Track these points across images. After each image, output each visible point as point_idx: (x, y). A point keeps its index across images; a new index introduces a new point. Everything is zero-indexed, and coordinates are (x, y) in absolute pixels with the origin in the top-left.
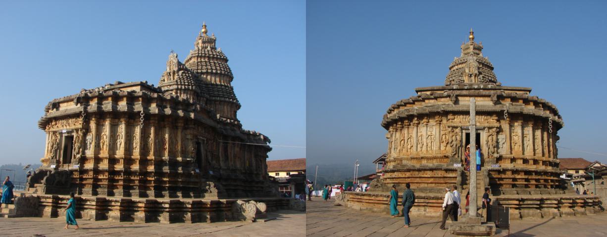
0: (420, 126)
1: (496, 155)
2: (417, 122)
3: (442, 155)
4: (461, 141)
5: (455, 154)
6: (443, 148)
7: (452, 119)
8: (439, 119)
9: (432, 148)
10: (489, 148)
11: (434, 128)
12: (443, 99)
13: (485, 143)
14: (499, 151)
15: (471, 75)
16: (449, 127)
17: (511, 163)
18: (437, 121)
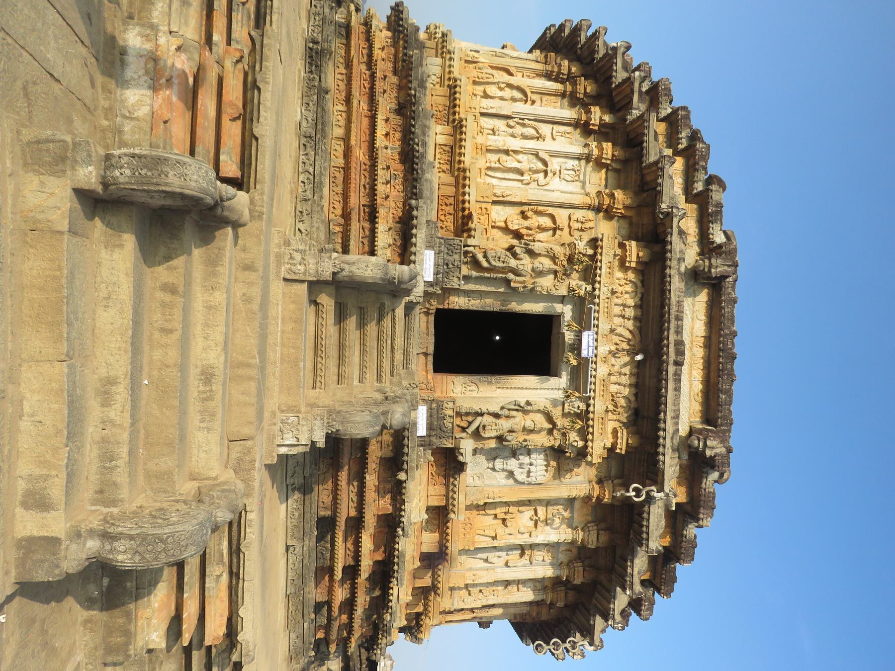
0: (576, 134)
1: (467, 445)
3: (473, 207)
4: (532, 294)
6: (499, 214)
10: (496, 416)
11: (575, 187)
13: (521, 397)
14: (481, 459)
18: (612, 196)
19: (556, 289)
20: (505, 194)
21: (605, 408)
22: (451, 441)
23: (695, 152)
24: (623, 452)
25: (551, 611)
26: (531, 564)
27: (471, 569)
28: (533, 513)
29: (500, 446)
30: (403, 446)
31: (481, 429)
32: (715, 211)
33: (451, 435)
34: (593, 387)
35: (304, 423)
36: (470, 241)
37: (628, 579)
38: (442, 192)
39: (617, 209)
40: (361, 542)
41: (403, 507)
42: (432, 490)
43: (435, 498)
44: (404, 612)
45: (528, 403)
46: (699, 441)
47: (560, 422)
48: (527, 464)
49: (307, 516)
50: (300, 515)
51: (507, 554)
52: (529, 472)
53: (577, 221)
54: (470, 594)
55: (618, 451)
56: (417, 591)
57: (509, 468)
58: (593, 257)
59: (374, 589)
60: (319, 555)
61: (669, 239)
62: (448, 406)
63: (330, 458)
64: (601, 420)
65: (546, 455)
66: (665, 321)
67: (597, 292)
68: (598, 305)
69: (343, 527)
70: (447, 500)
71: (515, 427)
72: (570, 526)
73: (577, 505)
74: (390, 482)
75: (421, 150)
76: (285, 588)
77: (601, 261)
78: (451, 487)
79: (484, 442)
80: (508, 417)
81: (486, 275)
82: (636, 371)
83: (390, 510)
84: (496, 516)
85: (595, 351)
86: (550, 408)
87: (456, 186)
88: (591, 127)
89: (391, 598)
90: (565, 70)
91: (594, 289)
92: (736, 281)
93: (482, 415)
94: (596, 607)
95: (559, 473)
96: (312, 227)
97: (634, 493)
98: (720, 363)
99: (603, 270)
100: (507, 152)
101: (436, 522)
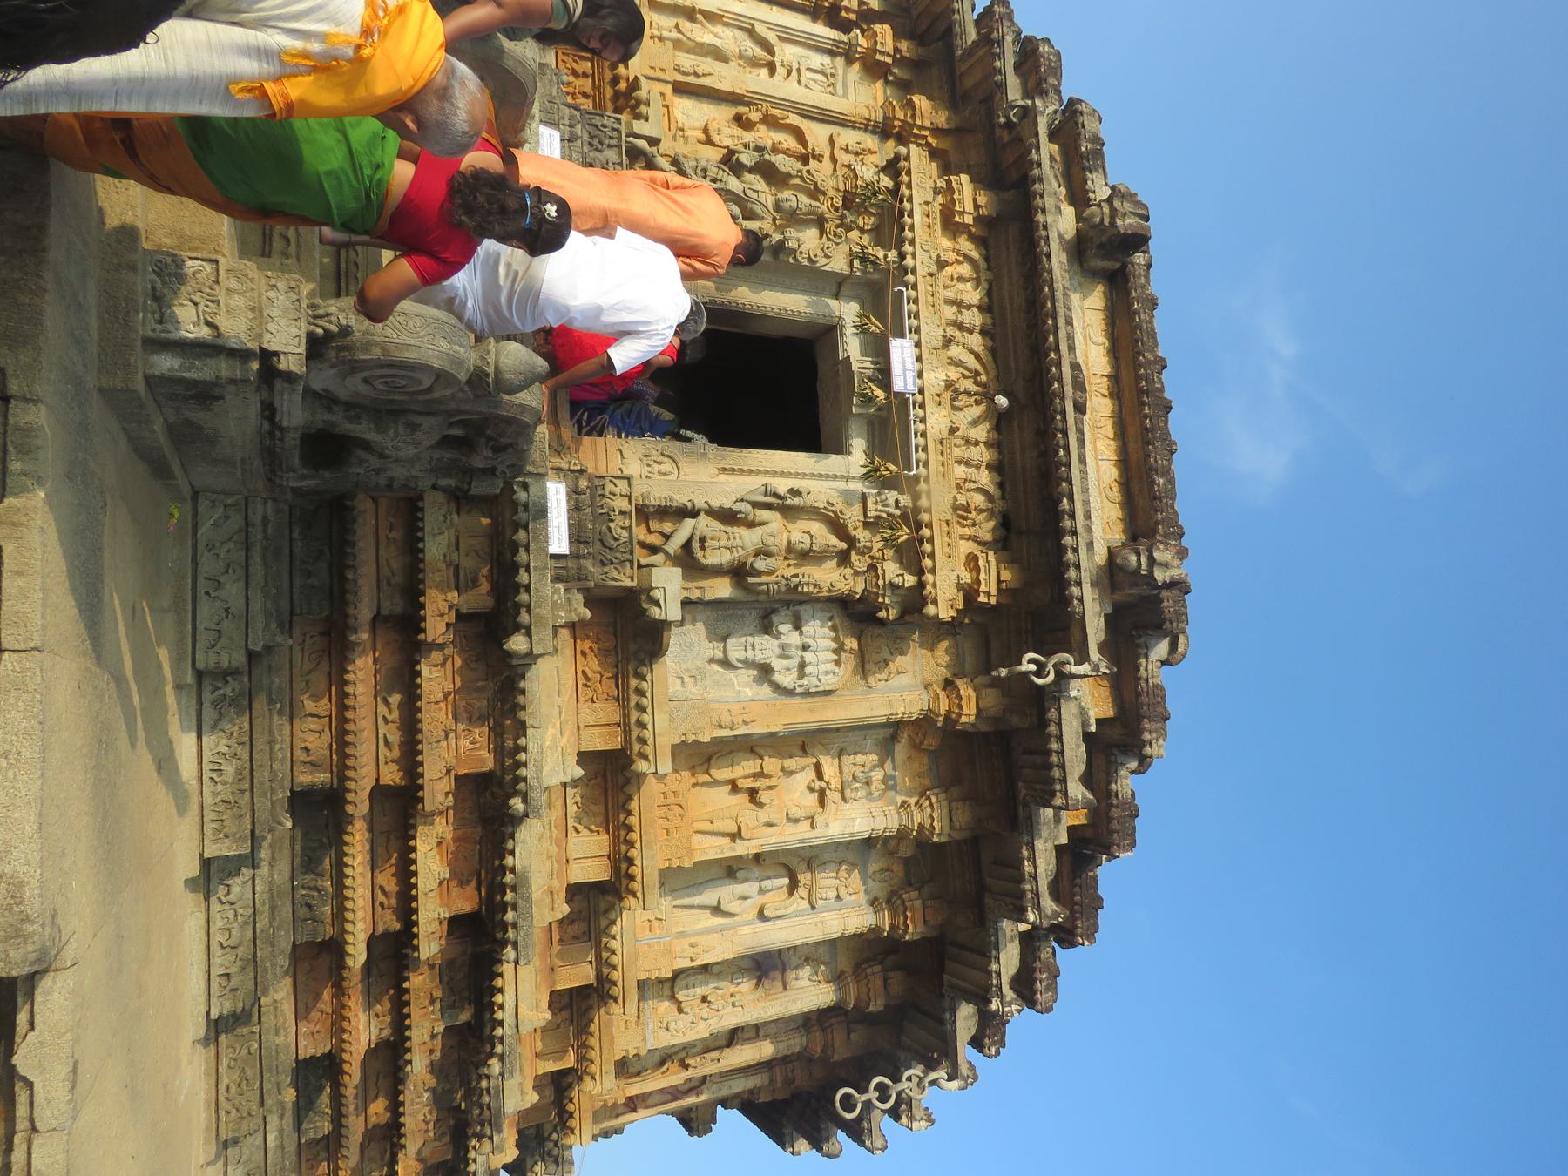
1: (669, 585)
10: (728, 517)
19: (827, 257)
20: (700, 71)
21: (951, 501)
22: (628, 571)
23: (1037, 61)
24: (993, 601)
25: (853, 1036)
26: (813, 908)
27: (682, 934)
28: (812, 774)
29: (740, 595)
30: (515, 568)
31: (696, 545)
32: (1092, 149)
33: (628, 556)
34: (922, 455)
35: (233, 284)
36: (639, 127)
37: (1028, 887)
39: (921, 128)
40: (414, 862)
41: (522, 741)
42: (588, 714)
43: (596, 730)
46: (1138, 555)
47: (862, 535)
48: (797, 648)
49: (262, 775)
50: (239, 772)
51: (761, 891)
52: (802, 665)
53: (847, 150)
54: (680, 1011)
55: (982, 599)
57: (760, 656)
58: (895, 192)
60: (303, 912)
61: (1035, 157)
62: (617, 490)
63: (321, 634)
64: (945, 528)
65: (834, 628)
66: (1047, 315)
67: (909, 261)
68: (915, 287)
70: (627, 733)
74: (480, 690)
76: (202, 999)
77: (910, 200)
78: (634, 699)
79: (700, 584)
80: (751, 525)
82: (994, 435)
83: (488, 762)
84: (734, 787)
85: (919, 382)
88: (843, 14)
89: (499, 1015)
91: (902, 256)
92: (1149, 265)
93: (693, 513)
94: (952, 986)
95: (865, 665)
97: (1033, 667)
98: (1146, 416)
99: (917, 217)
101: (600, 809)
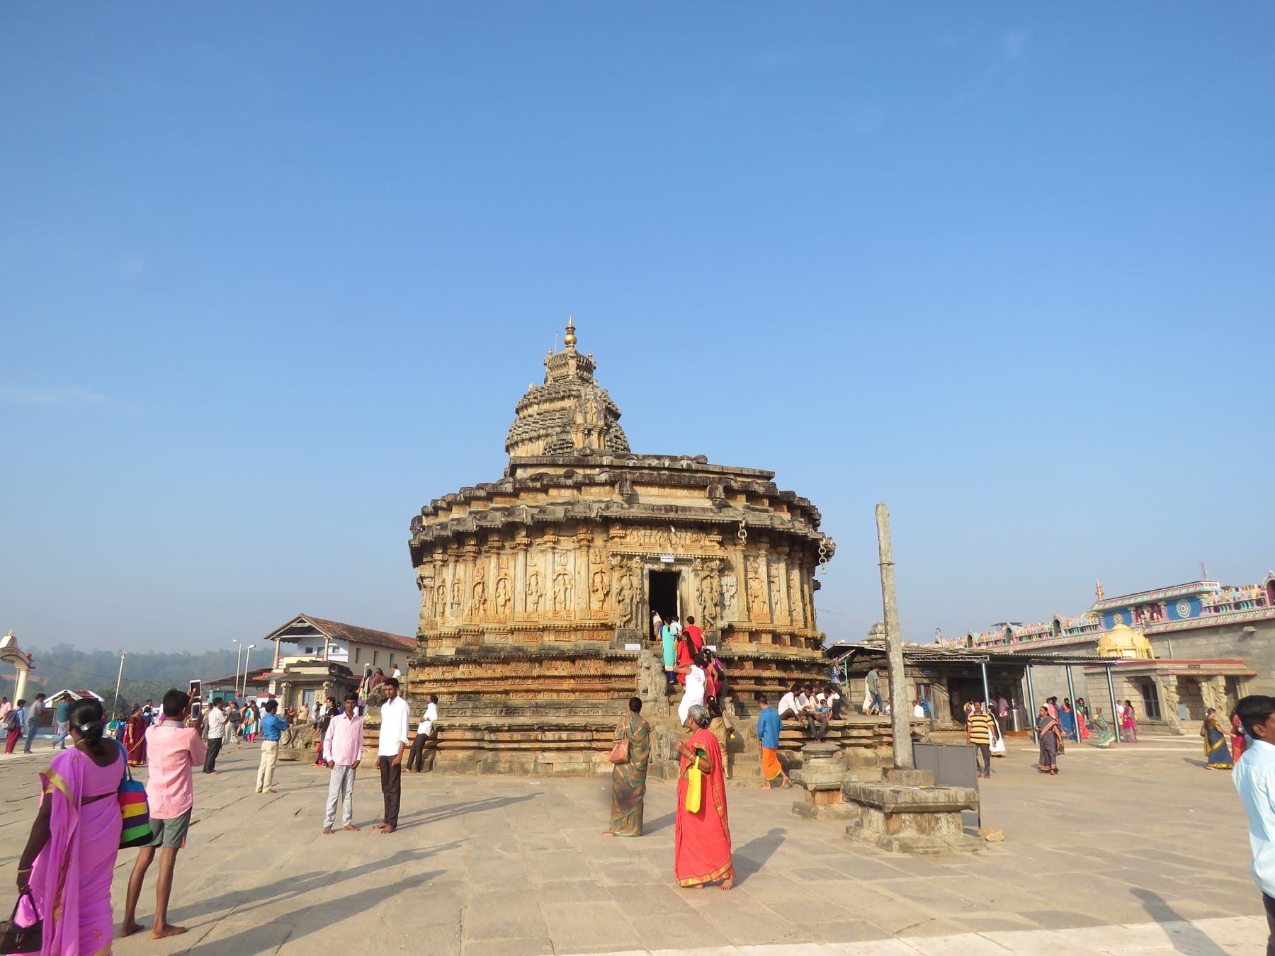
2: (525, 541)
5: (629, 621)
6: (595, 605)
7: (621, 537)
8: (589, 536)
9: (568, 603)
11: (571, 556)
12: (595, 490)
14: (725, 614)
15: (589, 431)
16: (614, 555)
17: (750, 641)
27: (781, 613)
31: (712, 616)
36: (618, 624)
38: (587, 638)
44: (804, 649)
45: (698, 590)
49: (755, 705)
52: (731, 586)
56: (794, 643)
59: (791, 668)
65: (722, 576)
67: (641, 554)
69: (760, 687)
71: (710, 598)
72: (758, 557)
73: (747, 553)
75: (573, 652)
81: (634, 615)
83: (751, 663)
84: (754, 602)
86: (699, 578)
87: (583, 630)
90: (473, 549)
96: (618, 707)
100: (555, 598)
